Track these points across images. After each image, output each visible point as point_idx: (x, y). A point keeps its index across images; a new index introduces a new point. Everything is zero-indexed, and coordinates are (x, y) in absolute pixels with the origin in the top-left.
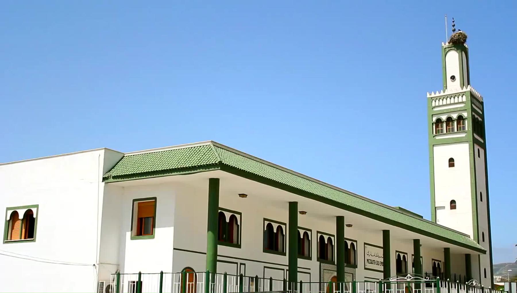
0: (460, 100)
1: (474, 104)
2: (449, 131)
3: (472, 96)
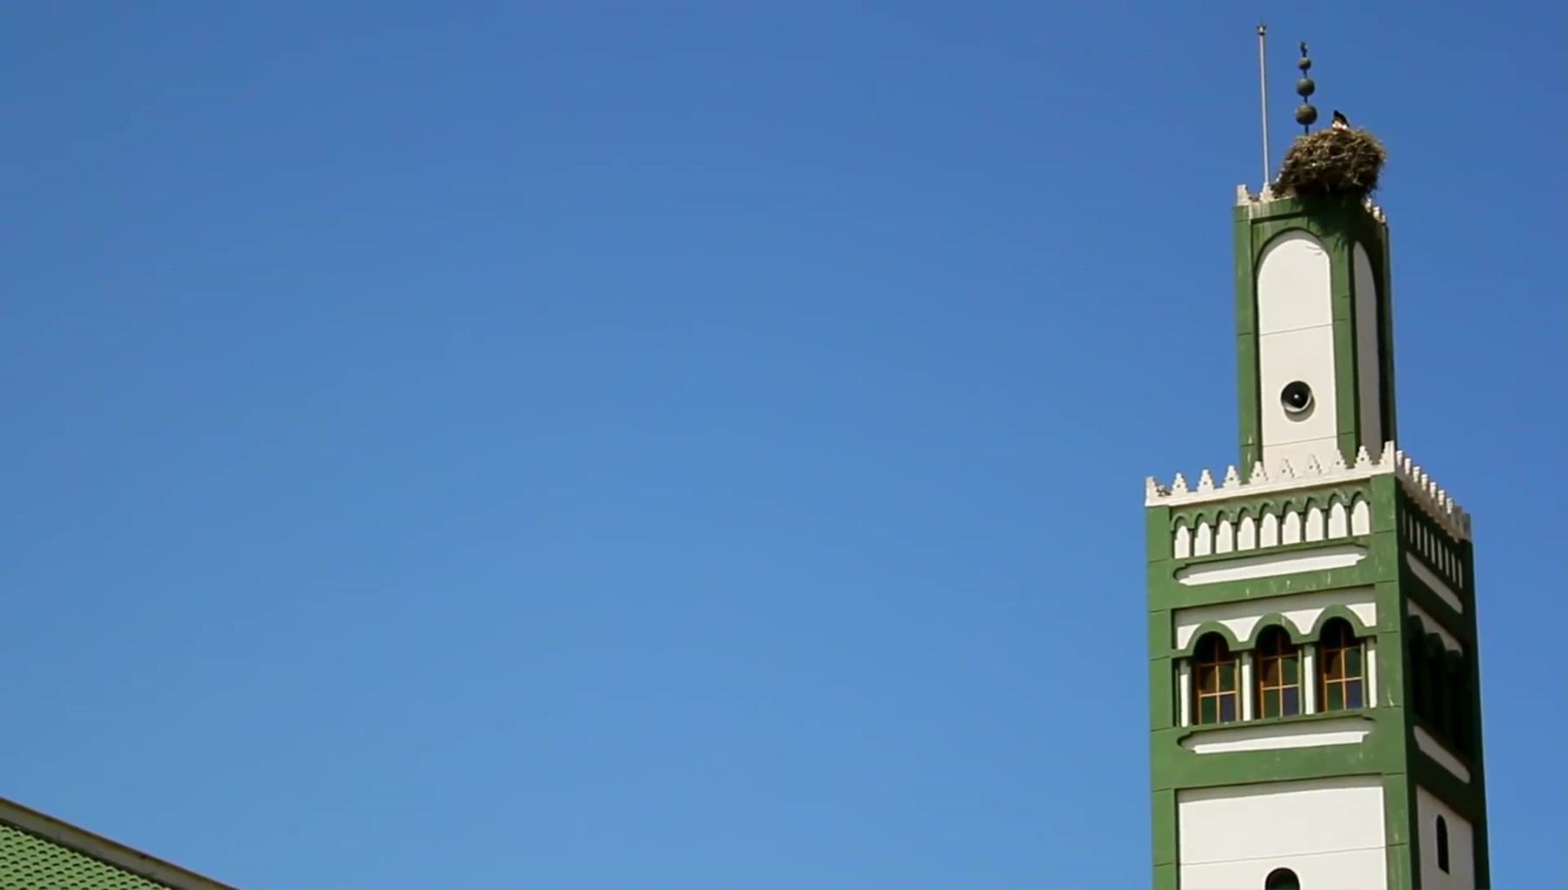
0: (1338, 530)
1: (1419, 556)
2: (1273, 711)
3: (1408, 506)
